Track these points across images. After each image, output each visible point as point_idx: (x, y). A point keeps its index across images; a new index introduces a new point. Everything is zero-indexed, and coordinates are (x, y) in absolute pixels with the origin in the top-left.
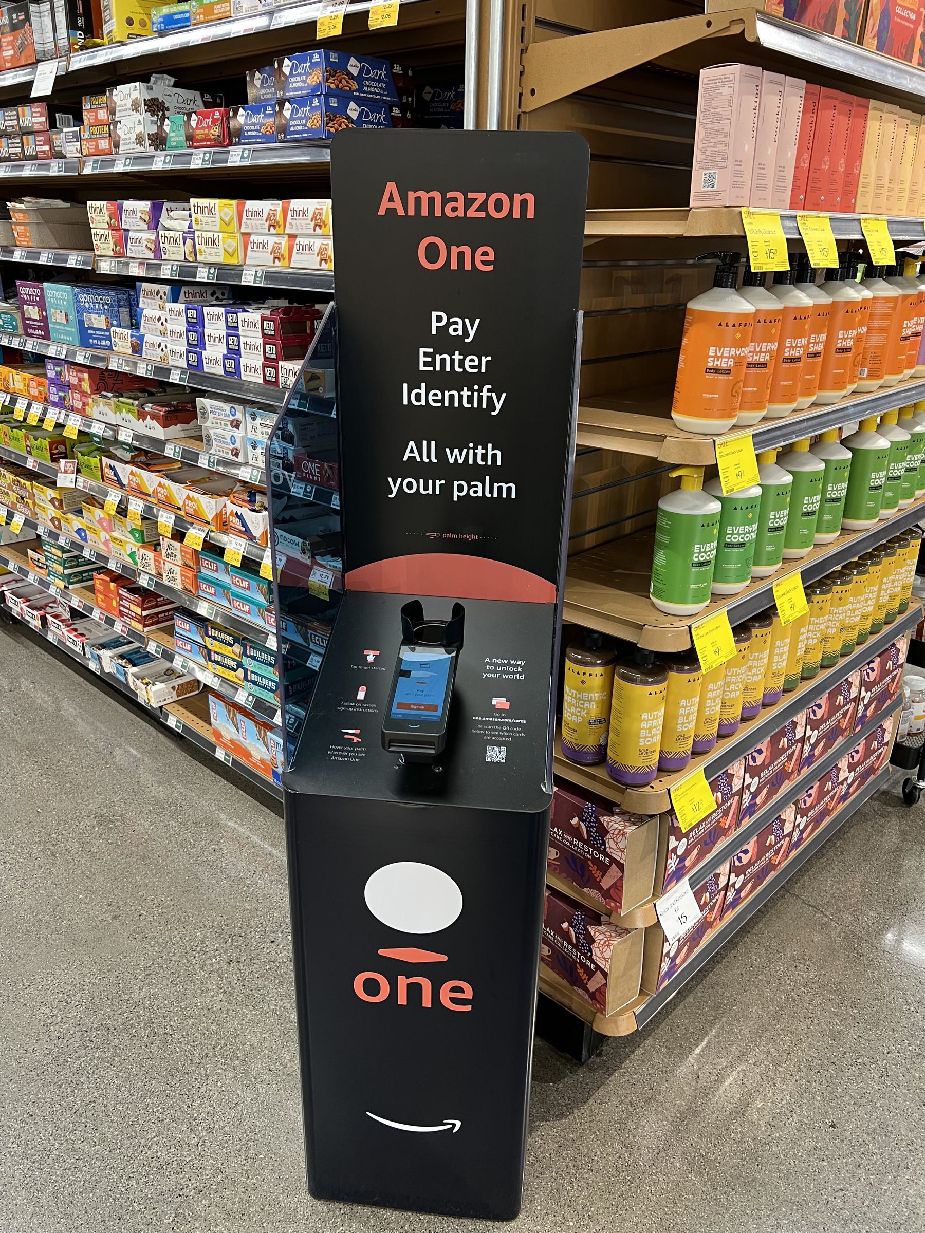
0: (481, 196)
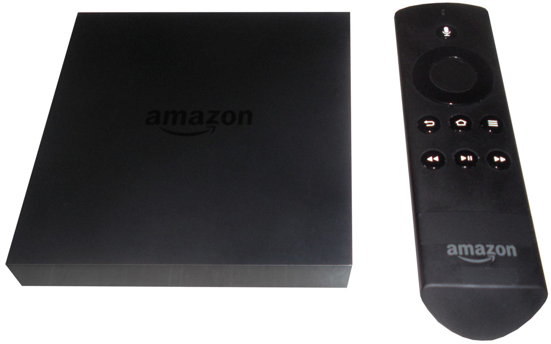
0: (491, 247)
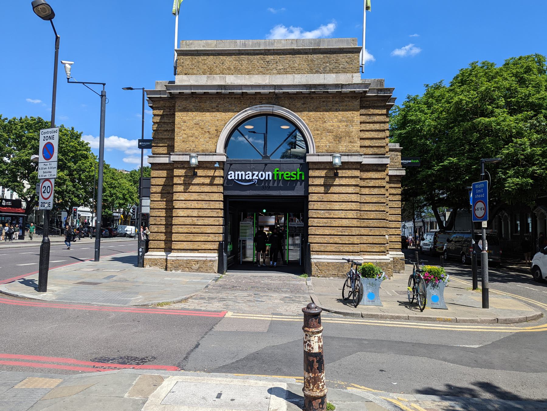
0: (256, 173)
